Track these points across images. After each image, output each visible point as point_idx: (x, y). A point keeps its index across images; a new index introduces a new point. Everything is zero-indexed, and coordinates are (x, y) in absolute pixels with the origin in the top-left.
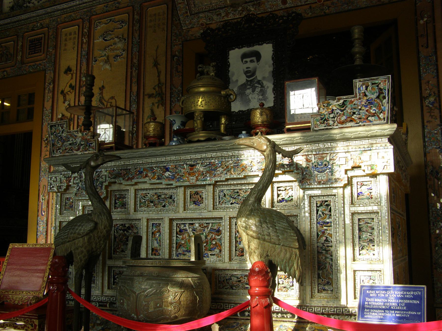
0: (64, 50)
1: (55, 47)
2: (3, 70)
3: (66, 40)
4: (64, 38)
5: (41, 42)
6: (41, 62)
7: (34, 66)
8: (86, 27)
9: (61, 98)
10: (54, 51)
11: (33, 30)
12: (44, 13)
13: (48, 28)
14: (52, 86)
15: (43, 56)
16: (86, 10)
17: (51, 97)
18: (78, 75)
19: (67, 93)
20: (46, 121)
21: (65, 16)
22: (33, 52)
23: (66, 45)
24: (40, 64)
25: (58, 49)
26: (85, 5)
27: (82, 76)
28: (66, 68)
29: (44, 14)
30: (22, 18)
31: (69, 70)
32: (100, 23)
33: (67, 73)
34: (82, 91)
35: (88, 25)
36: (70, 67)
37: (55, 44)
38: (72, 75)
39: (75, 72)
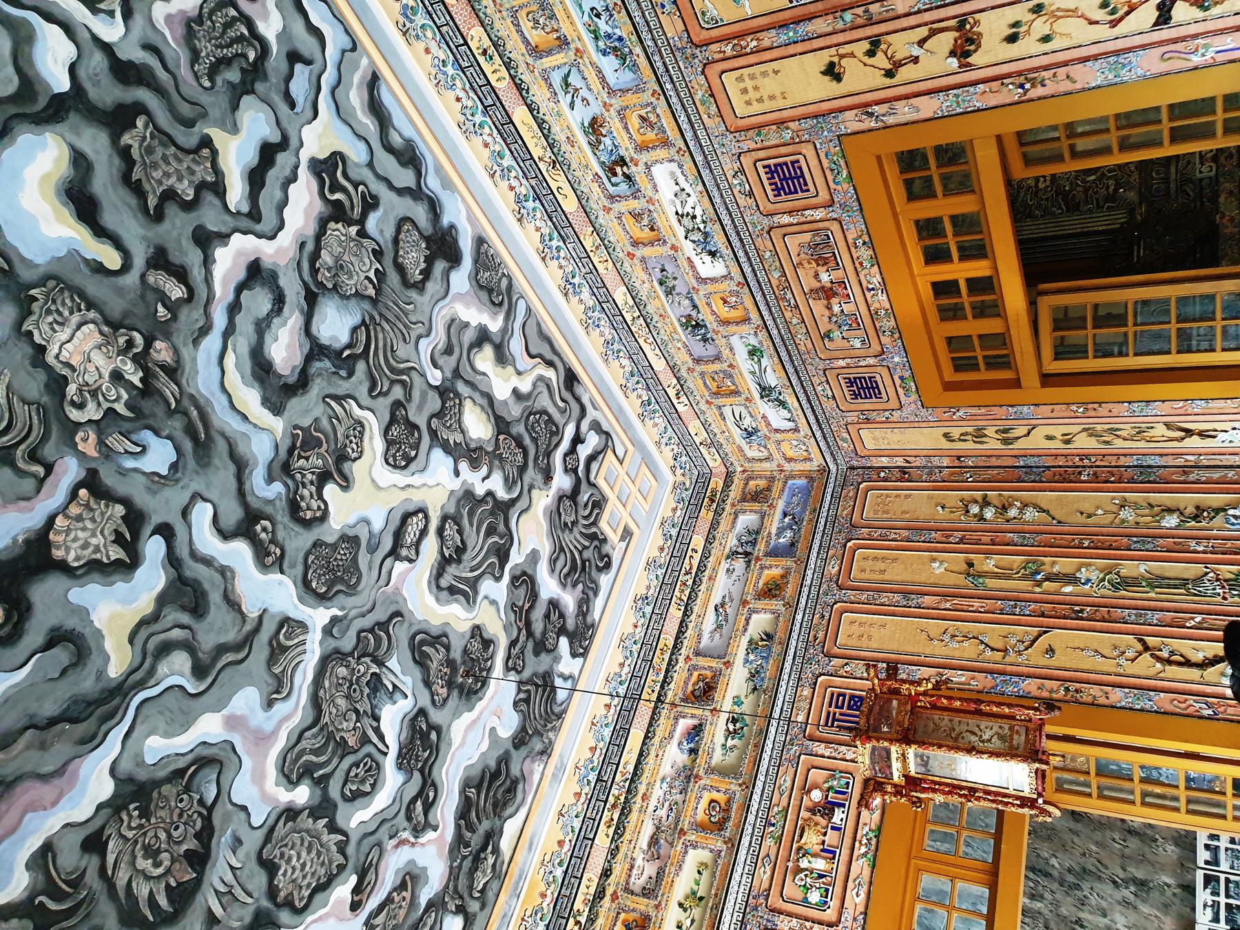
0: (784, 98)
1: (781, 123)
2: (853, 249)
3: (760, 100)
4: (756, 108)
5: (775, 165)
6: (822, 156)
7: (832, 170)
8: (720, 52)
9: (905, 73)
10: (791, 124)
11: (751, 194)
12: (708, 171)
13: (739, 157)
14: (876, 108)
15: (808, 150)
16: (680, 63)
17: (904, 102)
18: (840, 38)
19: (889, 59)
20: (969, 101)
21: (705, 117)
22: (801, 180)
23: (772, 98)
24: (826, 155)
25: (785, 114)
26: (670, 67)
27: (840, 25)
28: (827, 78)
29: (711, 171)
30: (730, 222)
31: (832, 72)
32: (703, 13)
33: (839, 74)
34: (880, 14)
35: (715, 47)
36: (823, 69)
37: (774, 127)
38: (842, 57)
39: (833, 50)
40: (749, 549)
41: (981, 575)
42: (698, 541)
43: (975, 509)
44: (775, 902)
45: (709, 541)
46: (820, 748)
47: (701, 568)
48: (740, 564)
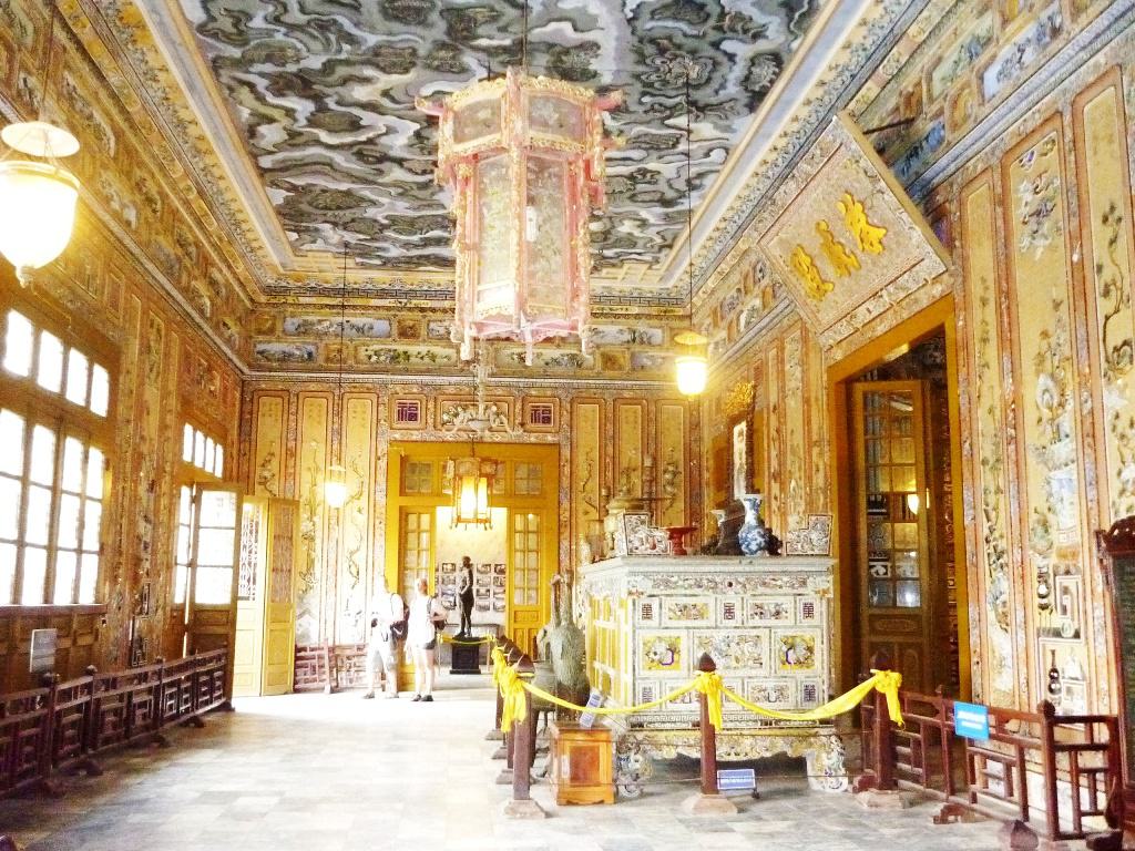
40: (638, 340)
41: (628, 477)
42: (635, 310)
43: (671, 468)
44: (441, 398)
45: (637, 316)
46: (519, 406)
47: (617, 316)
48: (627, 336)
